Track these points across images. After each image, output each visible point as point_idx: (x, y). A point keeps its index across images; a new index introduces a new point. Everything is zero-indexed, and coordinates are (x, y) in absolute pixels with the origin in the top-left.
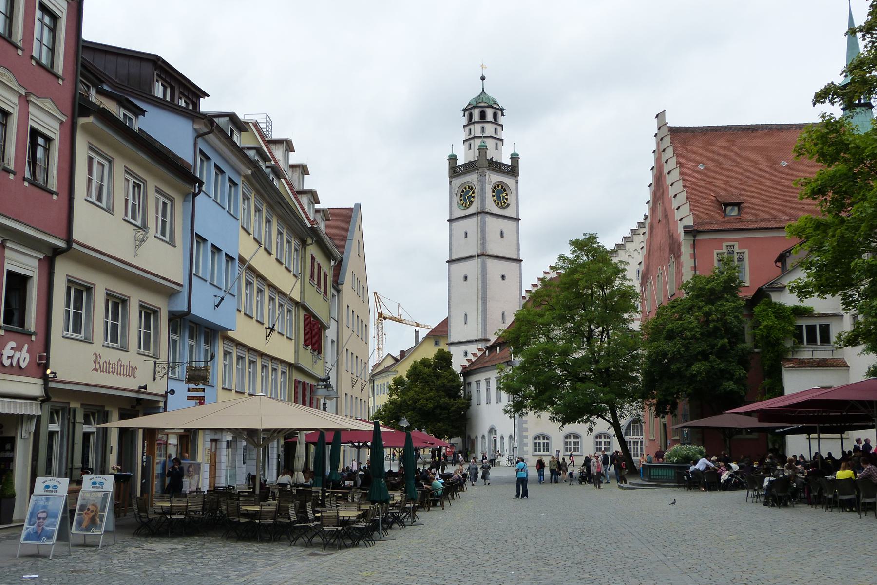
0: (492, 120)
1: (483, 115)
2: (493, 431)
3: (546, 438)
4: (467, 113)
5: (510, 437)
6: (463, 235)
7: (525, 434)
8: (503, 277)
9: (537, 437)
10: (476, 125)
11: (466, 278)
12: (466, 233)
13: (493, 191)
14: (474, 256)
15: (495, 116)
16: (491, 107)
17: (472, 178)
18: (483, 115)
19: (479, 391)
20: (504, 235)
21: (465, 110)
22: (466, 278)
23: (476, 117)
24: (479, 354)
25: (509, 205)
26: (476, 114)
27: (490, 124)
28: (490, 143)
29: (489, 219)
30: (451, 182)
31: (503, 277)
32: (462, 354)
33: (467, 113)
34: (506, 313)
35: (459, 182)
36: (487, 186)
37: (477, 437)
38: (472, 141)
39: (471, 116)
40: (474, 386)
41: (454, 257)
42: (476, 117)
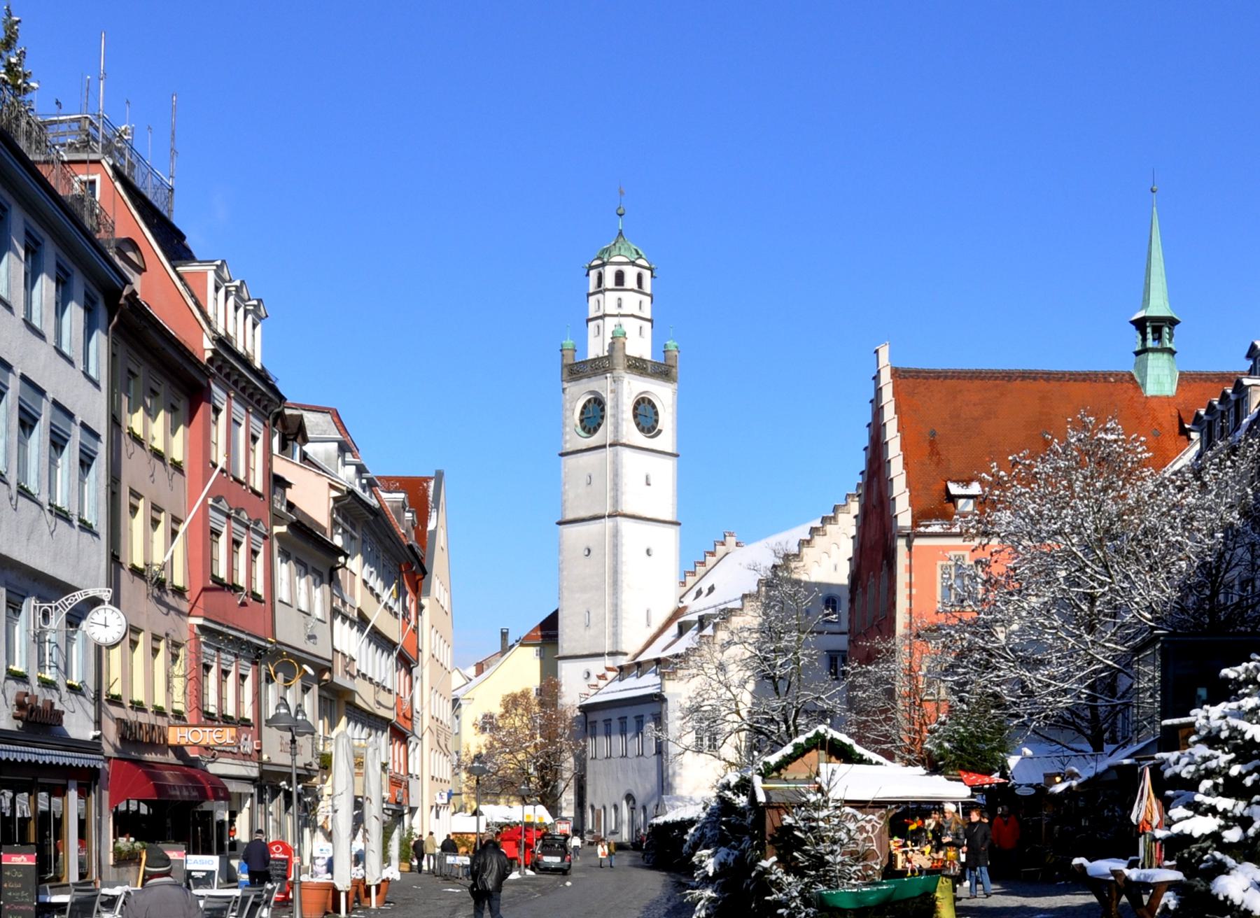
0: (635, 287)
1: (620, 278)
8: (648, 552)
13: (635, 408)
15: (640, 277)
17: (601, 385)
18: (620, 278)
23: (609, 281)
28: (630, 326)
29: (626, 454)
31: (648, 552)
32: (583, 675)
42: (609, 281)
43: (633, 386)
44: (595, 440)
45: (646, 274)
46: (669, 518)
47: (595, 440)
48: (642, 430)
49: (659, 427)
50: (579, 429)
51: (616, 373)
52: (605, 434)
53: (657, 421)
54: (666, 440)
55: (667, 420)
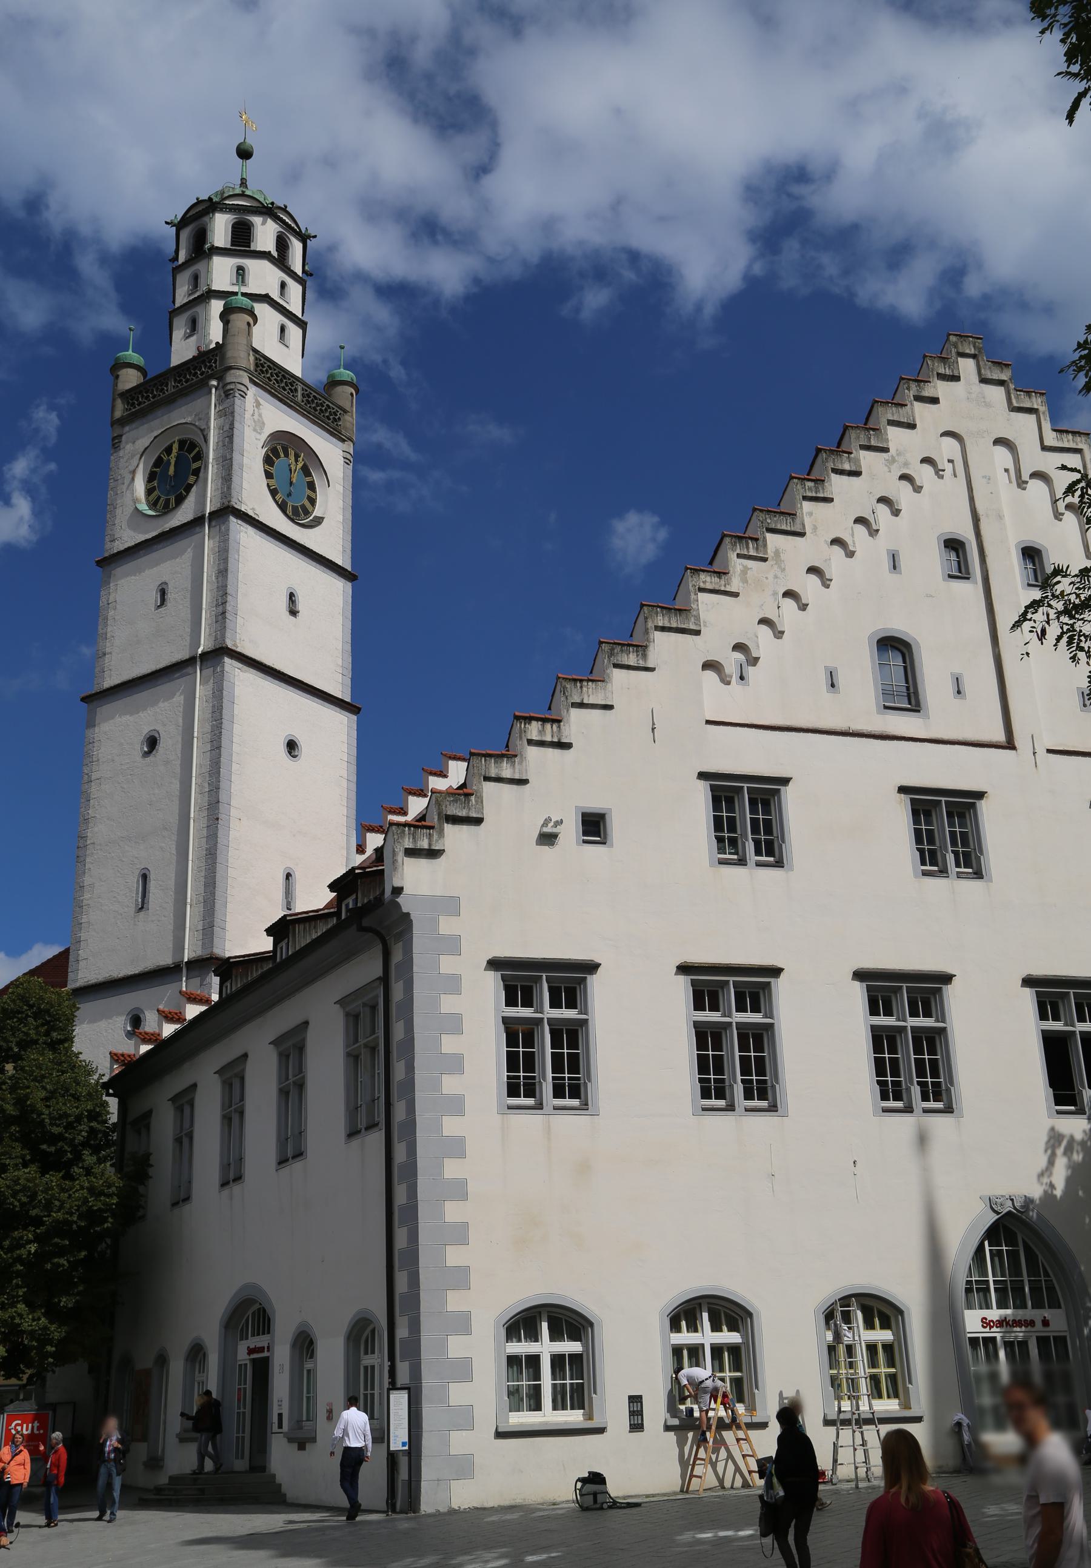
1: (242, 235)
2: (251, 1315)
3: (569, 1322)
4: (185, 234)
5: (360, 1335)
6: (154, 597)
7: (455, 1302)
8: (292, 746)
9: (523, 1324)
11: (152, 743)
12: (163, 593)
13: (268, 461)
14: (191, 661)
15: (282, 244)
16: (269, 211)
18: (242, 235)
19: (184, 1139)
20: (301, 606)
22: (152, 743)
24: (192, 1011)
25: (318, 521)
26: (220, 229)
27: (265, 264)
29: (245, 536)
31: (292, 746)
33: (185, 234)
37: (162, 1360)
38: (199, 309)
39: (201, 236)
40: (165, 1124)
43: (263, 417)
44: (184, 514)
45: (296, 247)
47: (184, 514)
49: (317, 512)
50: (143, 507)
51: (230, 377)
53: (313, 502)
54: (332, 537)
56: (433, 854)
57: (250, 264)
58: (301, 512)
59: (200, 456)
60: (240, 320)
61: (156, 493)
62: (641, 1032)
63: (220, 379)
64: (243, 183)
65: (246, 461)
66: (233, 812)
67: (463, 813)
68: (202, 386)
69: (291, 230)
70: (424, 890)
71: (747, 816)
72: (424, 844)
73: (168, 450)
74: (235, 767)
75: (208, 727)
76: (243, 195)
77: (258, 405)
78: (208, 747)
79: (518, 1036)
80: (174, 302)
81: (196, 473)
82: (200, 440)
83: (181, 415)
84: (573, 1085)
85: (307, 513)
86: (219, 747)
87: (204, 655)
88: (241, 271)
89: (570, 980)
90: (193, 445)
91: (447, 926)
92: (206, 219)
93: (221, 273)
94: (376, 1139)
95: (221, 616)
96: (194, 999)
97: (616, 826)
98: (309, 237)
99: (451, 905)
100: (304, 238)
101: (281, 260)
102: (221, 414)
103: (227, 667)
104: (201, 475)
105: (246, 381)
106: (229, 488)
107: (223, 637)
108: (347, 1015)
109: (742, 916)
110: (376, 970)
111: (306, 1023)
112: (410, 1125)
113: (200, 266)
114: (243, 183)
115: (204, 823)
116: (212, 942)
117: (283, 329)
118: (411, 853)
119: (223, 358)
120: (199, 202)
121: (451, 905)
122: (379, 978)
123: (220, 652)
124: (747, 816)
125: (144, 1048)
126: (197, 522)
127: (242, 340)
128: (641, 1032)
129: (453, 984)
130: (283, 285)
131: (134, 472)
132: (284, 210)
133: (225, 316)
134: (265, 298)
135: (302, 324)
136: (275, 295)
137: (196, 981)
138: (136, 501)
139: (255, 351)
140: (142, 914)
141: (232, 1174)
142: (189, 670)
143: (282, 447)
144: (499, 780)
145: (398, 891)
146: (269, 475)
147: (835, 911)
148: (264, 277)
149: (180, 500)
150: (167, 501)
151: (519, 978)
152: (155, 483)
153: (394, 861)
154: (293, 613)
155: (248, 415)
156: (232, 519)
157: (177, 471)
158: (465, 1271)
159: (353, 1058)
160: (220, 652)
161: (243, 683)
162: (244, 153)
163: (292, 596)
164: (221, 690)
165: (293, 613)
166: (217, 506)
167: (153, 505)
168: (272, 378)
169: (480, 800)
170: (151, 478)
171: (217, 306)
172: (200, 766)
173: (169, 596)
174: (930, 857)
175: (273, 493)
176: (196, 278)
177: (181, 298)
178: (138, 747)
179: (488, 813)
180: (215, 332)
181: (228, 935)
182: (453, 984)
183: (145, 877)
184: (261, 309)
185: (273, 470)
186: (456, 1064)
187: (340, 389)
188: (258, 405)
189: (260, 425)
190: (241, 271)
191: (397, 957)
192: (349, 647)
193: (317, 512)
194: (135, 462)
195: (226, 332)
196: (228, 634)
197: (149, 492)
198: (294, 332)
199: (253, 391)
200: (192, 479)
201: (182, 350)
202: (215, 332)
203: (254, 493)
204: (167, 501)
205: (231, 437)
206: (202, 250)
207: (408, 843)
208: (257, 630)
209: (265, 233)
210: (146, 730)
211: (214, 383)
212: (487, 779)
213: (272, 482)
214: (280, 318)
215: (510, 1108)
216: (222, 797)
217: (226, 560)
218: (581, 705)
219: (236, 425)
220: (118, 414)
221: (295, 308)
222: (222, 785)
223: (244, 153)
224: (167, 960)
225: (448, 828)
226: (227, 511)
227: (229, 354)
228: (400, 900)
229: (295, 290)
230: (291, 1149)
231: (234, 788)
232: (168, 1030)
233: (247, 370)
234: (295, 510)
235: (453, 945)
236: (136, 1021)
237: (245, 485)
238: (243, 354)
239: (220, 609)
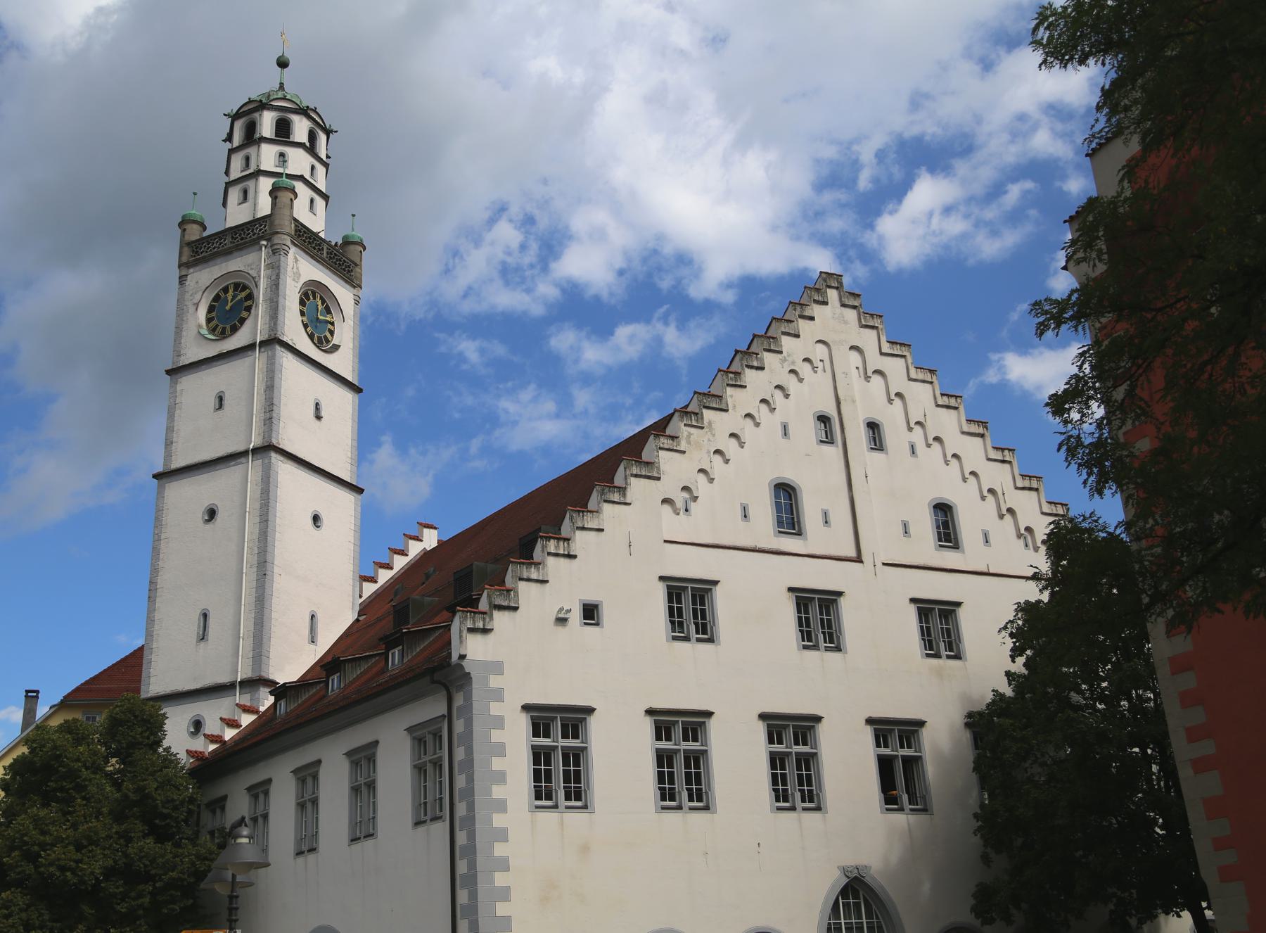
1: (283, 129)
4: (239, 125)
6: (212, 402)
8: (316, 519)
10: (264, 146)
11: (212, 514)
13: (302, 303)
14: (244, 454)
15: (312, 136)
16: (304, 112)
18: (283, 129)
20: (323, 414)
21: (235, 117)
22: (212, 514)
25: (336, 348)
27: (300, 153)
29: (287, 361)
30: (182, 280)
31: (316, 519)
34: (319, 617)
35: (204, 277)
36: (289, 281)
39: (251, 129)
41: (175, 465)
43: (302, 269)
45: (322, 137)
46: (347, 478)
48: (311, 337)
49: (335, 341)
50: (205, 332)
51: (276, 239)
52: (254, 328)
53: (332, 333)
55: (345, 333)
56: (485, 631)
57: (290, 151)
58: (323, 340)
59: (250, 297)
60: (284, 197)
61: (215, 322)
62: (621, 756)
63: (268, 240)
64: (282, 87)
65: (287, 303)
66: (276, 570)
67: (505, 603)
68: (255, 243)
69: (320, 127)
70: (480, 657)
71: (690, 607)
72: (480, 625)
73: (226, 290)
74: (277, 535)
75: (258, 506)
76: (284, 99)
77: (296, 260)
78: (258, 520)
79: (540, 757)
80: (227, 173)
81: (248, 309)
82: (252, 286)
83: (236, 264)
84: (577, 793)
85: (328, 341)
86: (267, 521)
87: (256, 451)
88: (282, 155)
89: (574, 719)
90: (245, 287)
91: (495, 682)
92: (256, 115)
93: (267, 156)
94: (441, 829)
95: (269, 419)
96: (247, 710)
97: (606, 613)
98: (332, 131)
99: (498, 667)
100: (328, 132)
101: (311, 149)
102: (268, 266)
103: (273, 460)
104: (253, 311)
105: (289, 243)
106: (275, 324)
107: (270, 436)
108: (414, 738)
109: (686, 677)
110: (443, 710)
111: (377, 742)
112: (470, 819)
113: (252, 151)
114: (282, 87)
115: (254, 576)
116: (260, 666)
117: (312, 201)
118: (472, 630)
119: (272, 224)
120: (250, 101)
121: (498, 667)
122: (443, 716)
123: (267, 448)
124: (690, 607)
125: (212, 747)
126: (251, 347)
127: (286, 212)
128: (621, 756)
129: (499, 722)
130: (313, 168)
131: (197, 305)
132: (315, 111)
133: (274, 193)
134: (301, 178)
135: (325, 197)
136: (307, 176)
137: (248, 696)
138: (200, 326)
139: (295, 220)
140: (202, 644)
141: (307, 846)
142: (243, 460)
143: (312, 294)
144: (529, 580)
145: (462, 657)
146: (302, 313)
147: (746, 674)
148: (299, 162)
149: (234, 329)
150: (224, 329)
151: (542, 718)
152: (214, 314)
153: (461, 637)
154: (319, 417)
155: (289, 269)
156: (278, 347)
157: (230, 308)
158: (508, 919)
159: (420, 769)
160: (267, 448)
161: (285, 471)
162: (282, 64)
163: (317, 404)
164: (268, 477)
165: (319, 417)
166: (265, 337)
167: (213, 331)
168: (307, 240)
169: (517, 594)
170: (211, 309)
171: (266, 184)
172: (251, 533)
173: (226, 402)
174: (807, 637)
175: (306, 326)
176: (247, 159)
177: (236, 173)
178: (200, 515)
179: (522, 603)
180: (264, 206)
181: (271, 662)
182: (499, 722)
183: (205, 616)
184: (300, 187)
185: (305, 309)
186: (501, 778)
187: (352, 247)
188: (296, 260)
189: (297, 275)
190: (282, 155)
191: (459, 701)
192: (355, 444)
193: (335, 341)
194: (198, 297)
195: (274, 205)
196: (274, 435)
197: (209, 320)
198: (320, 202)
199: (293, 251)
200: (244, 314)
201: (237, 215)
202: (264, 206)
203: (293, 329)
204: (224, 329)
205: (277, 285)
206: (252, 137)
207: (470, 625)
208: (294, 433)
209: (300, 129)
210: (206, 504)
211: (264, 243)
212: (521, 579)
213: (305, 318)
214: (311, 193)
215: (537, 807)
216: (269, 558)
217: (272, 379)
218: (583, 528)
219: (282, 276)
220: (184, 259)
221: (321, 185)
222: (269, 549)
223: (282, 64)
224: (224, 679)
225: (496, 614)
226: (273, 341)
227: (277, 222)
228: (464, 663)
229: (321, 170)
230: (362, 830)
231: (277, 551)
232: (229, 734)
233: (289, 235)
234: (319, 338)
235: (498, 695)
236: (198, 725)
237: (287, 321)
238: (287, 223)
239: (268, 416)
